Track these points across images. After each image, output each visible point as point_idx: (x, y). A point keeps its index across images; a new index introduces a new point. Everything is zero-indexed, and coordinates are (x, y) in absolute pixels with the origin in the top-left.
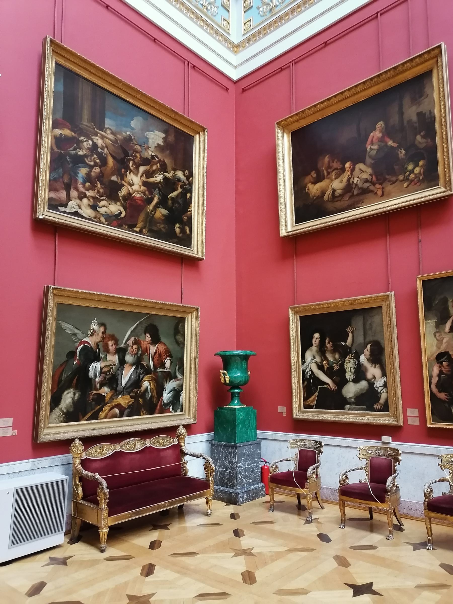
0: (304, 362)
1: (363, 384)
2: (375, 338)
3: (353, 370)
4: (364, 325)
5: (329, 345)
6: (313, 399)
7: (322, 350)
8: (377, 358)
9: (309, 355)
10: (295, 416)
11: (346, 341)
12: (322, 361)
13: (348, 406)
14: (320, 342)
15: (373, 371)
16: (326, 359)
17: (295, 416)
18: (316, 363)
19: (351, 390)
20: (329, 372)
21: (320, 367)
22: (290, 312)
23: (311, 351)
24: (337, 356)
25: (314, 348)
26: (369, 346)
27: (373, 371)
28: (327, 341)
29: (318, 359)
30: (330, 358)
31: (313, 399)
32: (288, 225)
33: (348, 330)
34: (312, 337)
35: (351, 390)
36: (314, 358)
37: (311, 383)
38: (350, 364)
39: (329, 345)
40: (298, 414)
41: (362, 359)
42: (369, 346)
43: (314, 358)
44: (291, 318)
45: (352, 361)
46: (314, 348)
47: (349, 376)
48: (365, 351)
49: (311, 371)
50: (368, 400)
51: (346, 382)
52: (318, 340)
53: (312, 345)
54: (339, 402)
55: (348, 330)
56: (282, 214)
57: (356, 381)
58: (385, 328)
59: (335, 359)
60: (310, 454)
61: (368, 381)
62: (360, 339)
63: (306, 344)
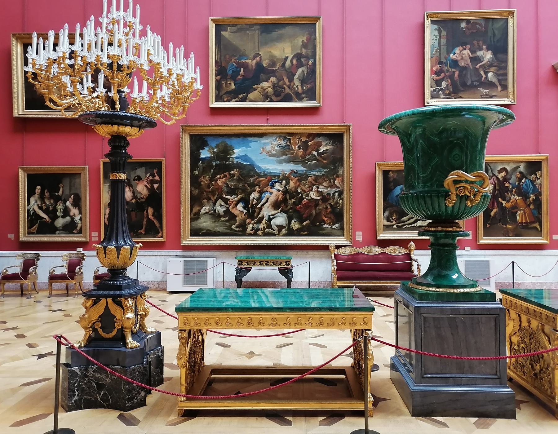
0: (27, 204)
1: (68, 218)
2: (76, 192)
3: (62, 210)
4: (70, 183)
5: (47, 194)
6: (35, 228)
7: (42, 197)
8: (77, 203)
9: (32, 200)
10: (21, 240)
11: (58, 193)
12: (42, 204)
13: (58, 232)
14: (41, 192)
15: (74, 211)
16: (45, 203)
17: (21, 240)
18: (38, 205)
19: (60, 222)
20: (46, 211)
21: (40, 208)
22: (20, 170)
23: (35, 197)
24: (52, 201)
25: (37, 196)
26: (72, 196)
27: (74, 211)
28: (46, 191)
29: (39, 203)
30: (48, 203)
31: (35, 228)
32: (19, 109)
33: (60, 185)
34: (35, 188)
35: (60, 222)
36: (36, 202)
37: (33, 218)
38: (60, 207)
39: (47, 194)
40: (22, 238)
41: (68, 203)
42: (72, 196)
43: (36, 202)
44: (20, 174)
45: (61, 204)
46: (37, 196)
47: (59, 214)
48: (70, 199)
49: (34, 210)
50: (70, 228)
51: (58, 217)
52: (39, 191)
53: (35, 193)
54: (52, 229)
55: (60, 185)
56: (15, 100)
57: (63, 217)
58: (82, 187)
59: (51, 203)
60: (31, 261)
61: (71, 217)
62: (67, 192)
63: (31, 193)
